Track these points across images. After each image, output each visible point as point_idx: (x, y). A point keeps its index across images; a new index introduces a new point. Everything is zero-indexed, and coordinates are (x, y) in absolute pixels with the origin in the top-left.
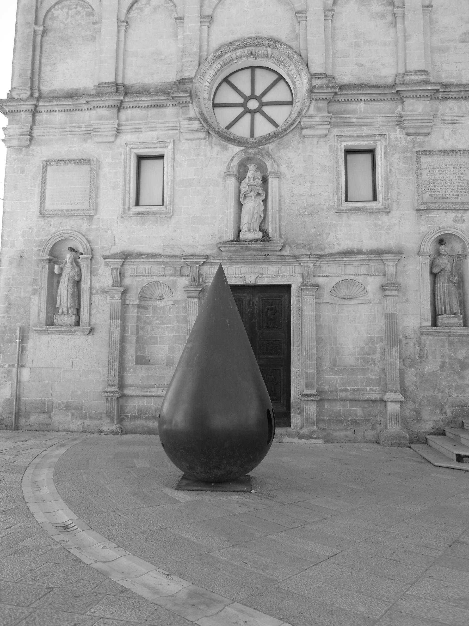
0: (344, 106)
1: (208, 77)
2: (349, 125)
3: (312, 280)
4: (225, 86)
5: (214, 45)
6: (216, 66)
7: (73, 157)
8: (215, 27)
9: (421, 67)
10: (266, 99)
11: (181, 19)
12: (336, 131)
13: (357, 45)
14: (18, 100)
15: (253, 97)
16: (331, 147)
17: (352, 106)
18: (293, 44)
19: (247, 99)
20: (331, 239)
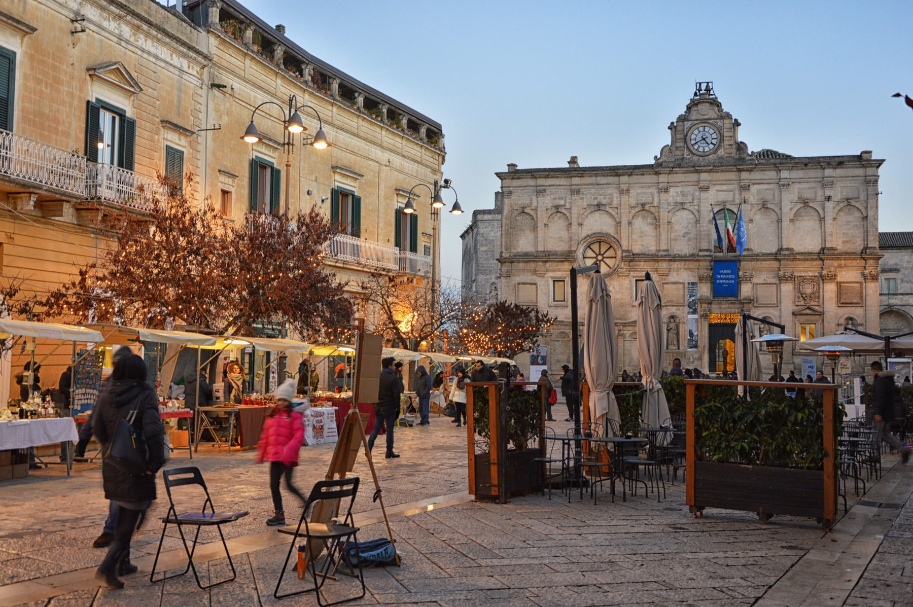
0: (635, 263)
1: (582, 249)
2: (637, 271)
3: (622, 332)
4: (588, 249)
5: (584, 235)
6: (585, 244)
7: (528, 281)
8: (584, 227)
9: (666, 248)
10: (605, 256)
11: (571, 224)
12: (632, 274)
13: (642, 237)
14: (506, 258)
15: (600, 254)
16: (630, 281)
17: (639, 263)
18: (616, 236)
19: (597, 255)
20: (629, 316)
